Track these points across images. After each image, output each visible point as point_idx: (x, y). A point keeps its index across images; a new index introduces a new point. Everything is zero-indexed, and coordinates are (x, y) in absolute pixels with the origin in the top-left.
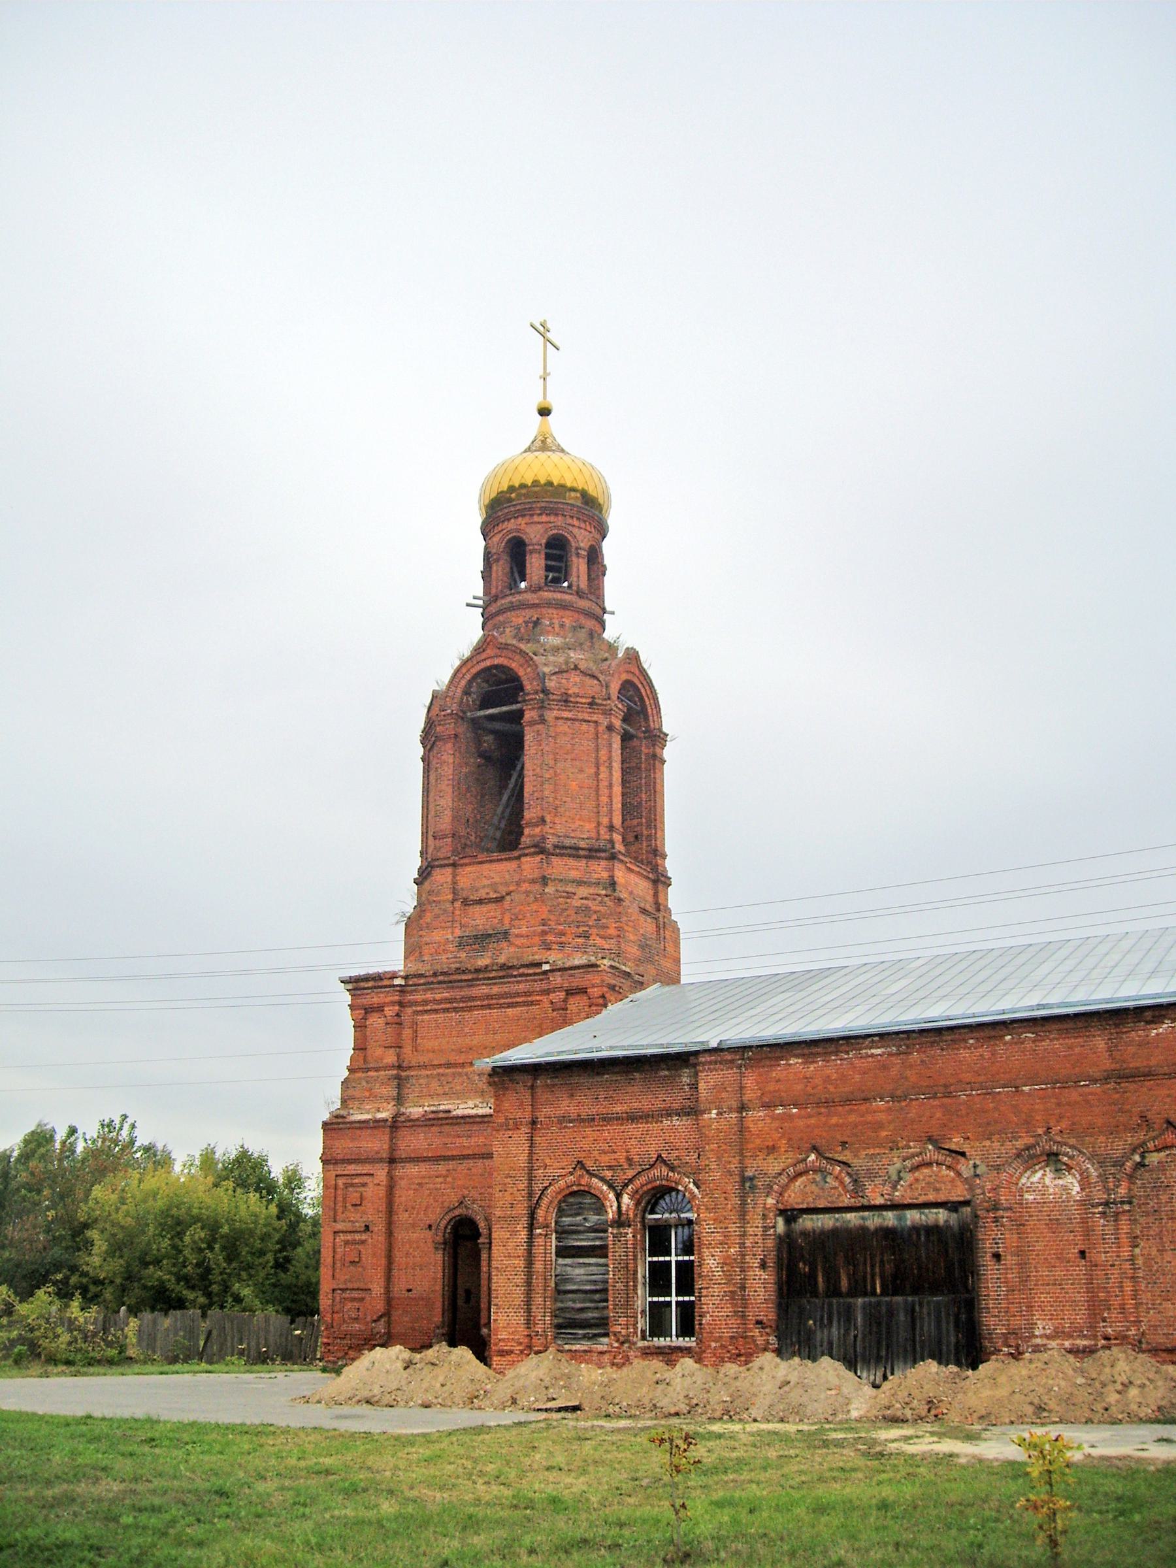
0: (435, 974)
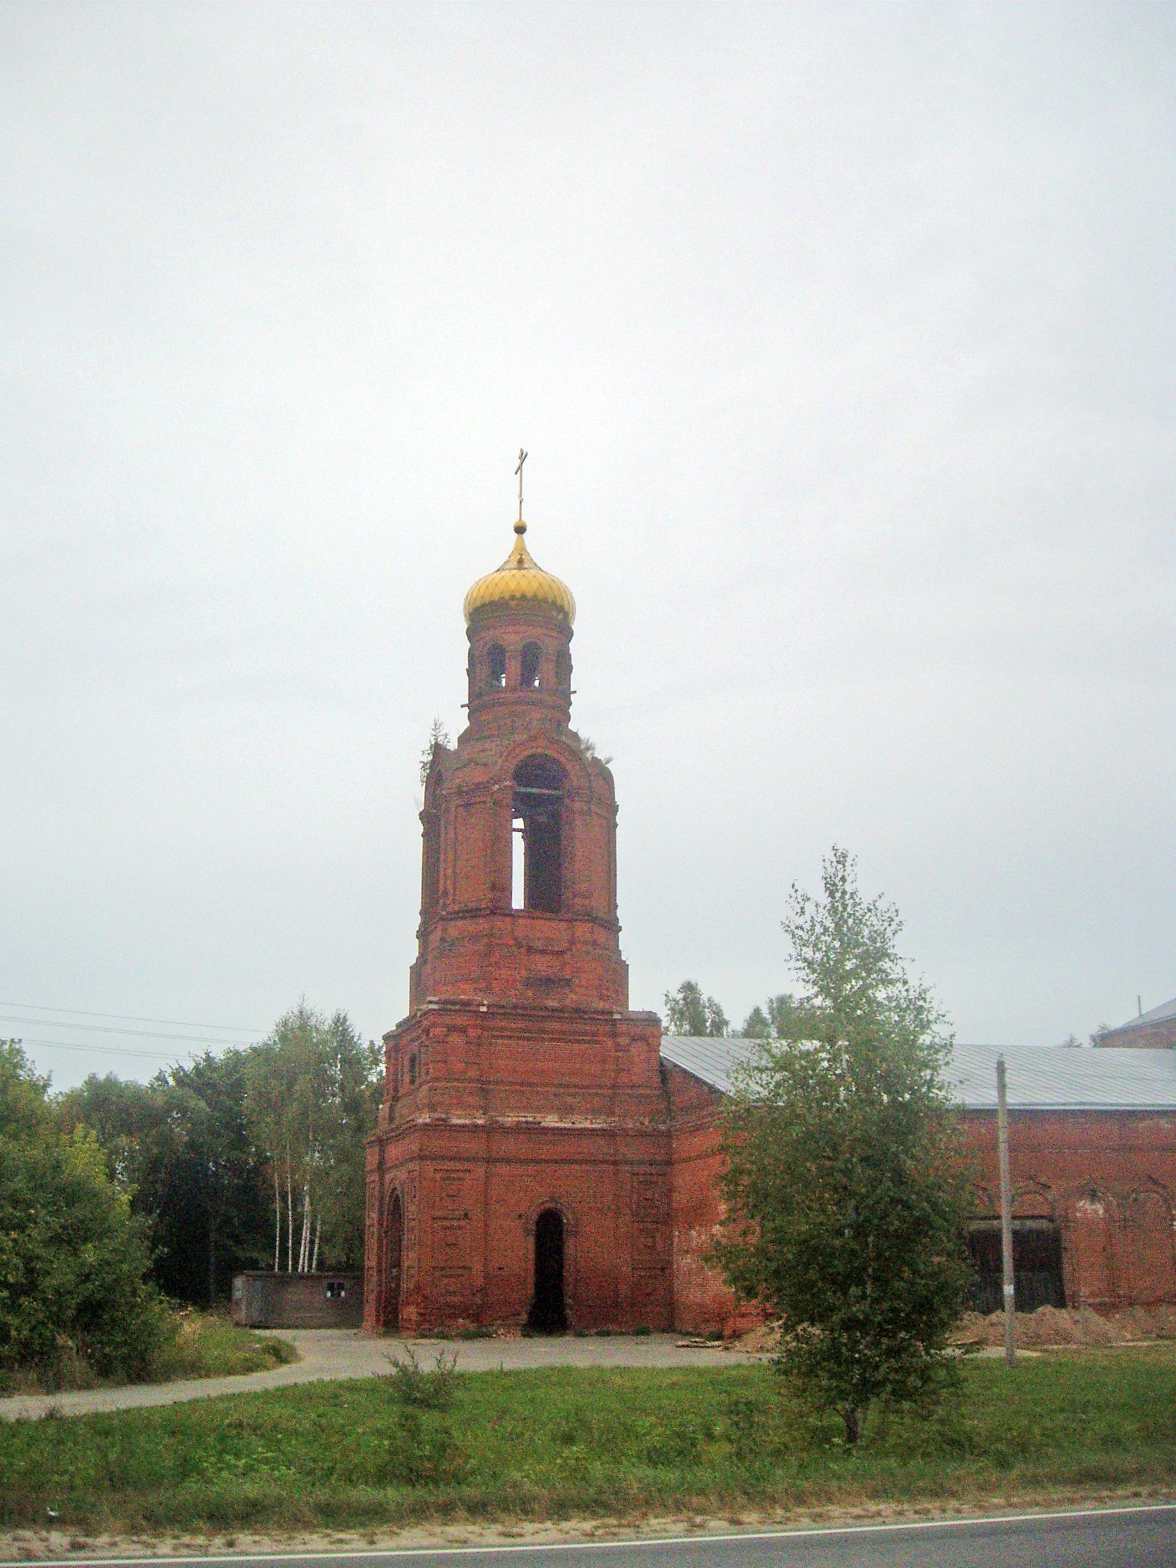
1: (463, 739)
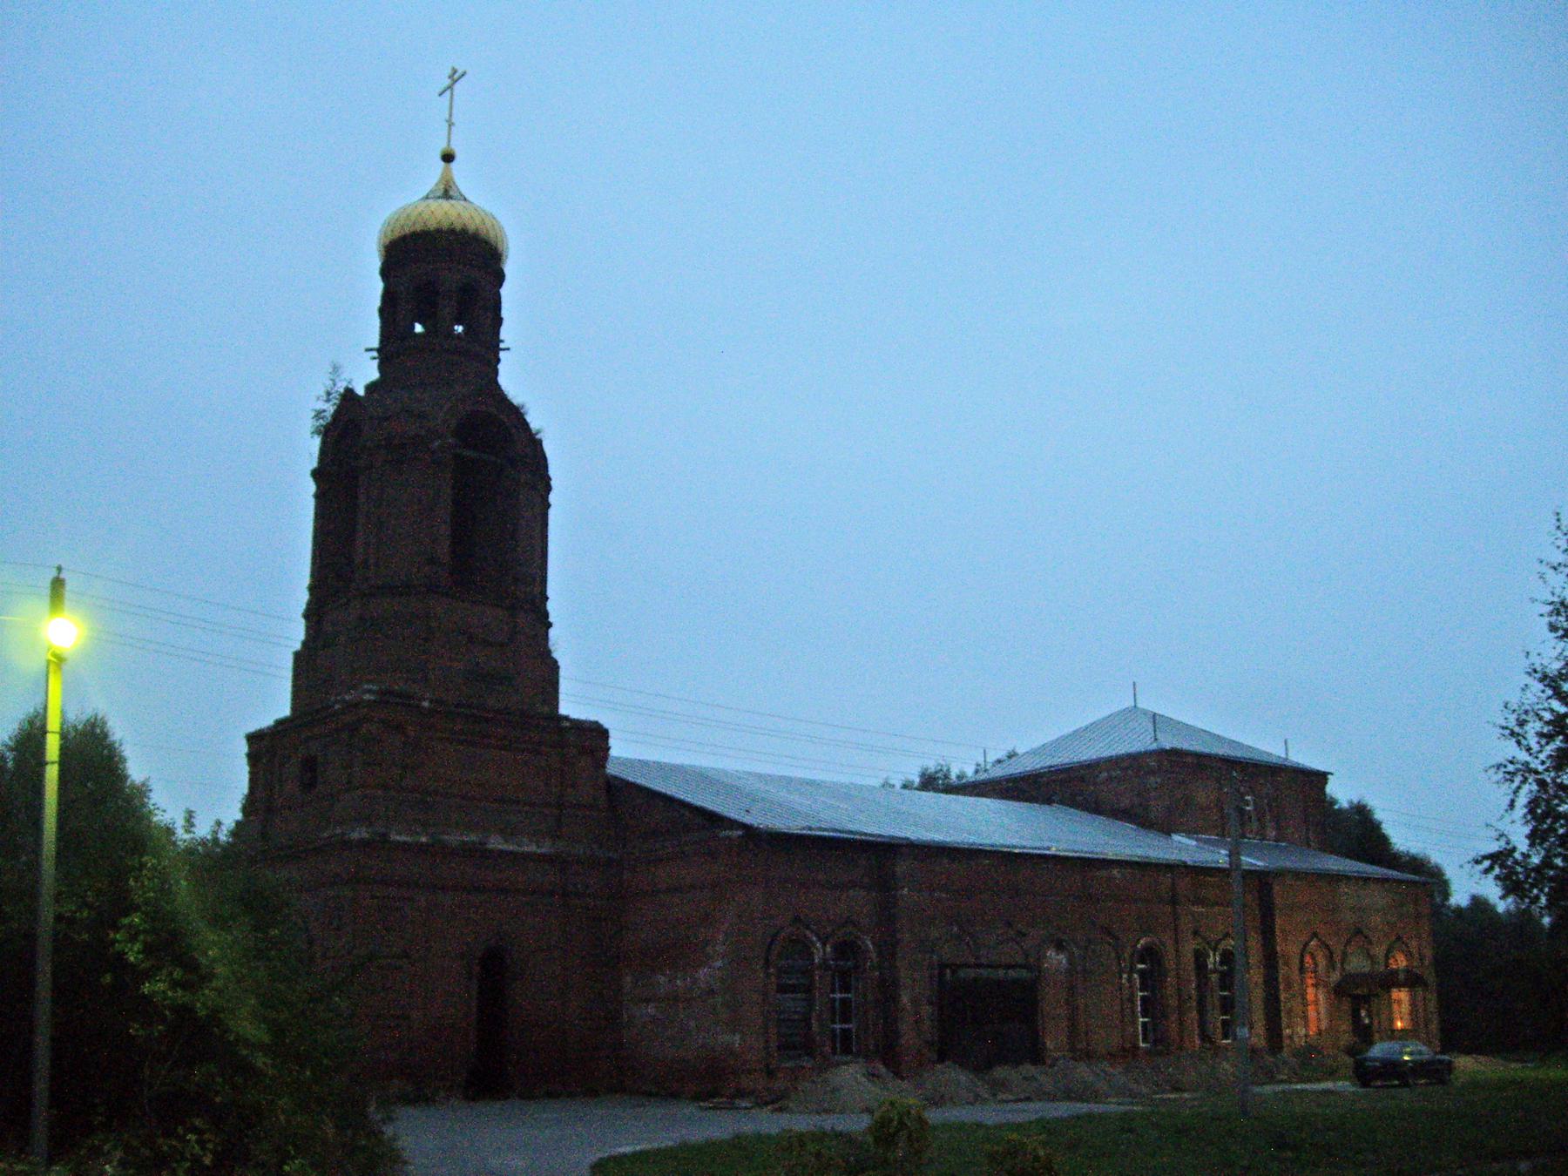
0: (457, 706)
1: (371, 388)
